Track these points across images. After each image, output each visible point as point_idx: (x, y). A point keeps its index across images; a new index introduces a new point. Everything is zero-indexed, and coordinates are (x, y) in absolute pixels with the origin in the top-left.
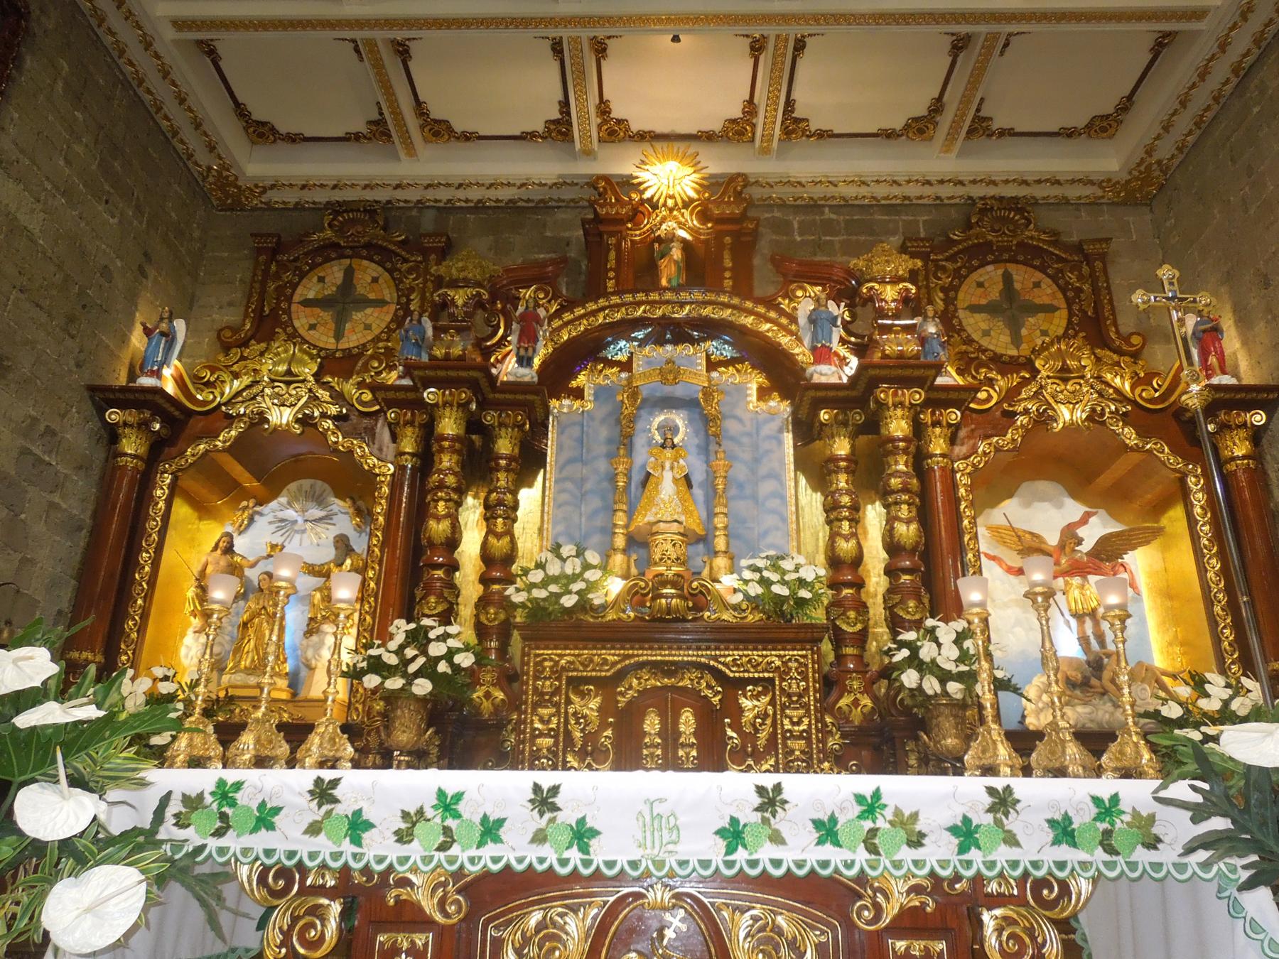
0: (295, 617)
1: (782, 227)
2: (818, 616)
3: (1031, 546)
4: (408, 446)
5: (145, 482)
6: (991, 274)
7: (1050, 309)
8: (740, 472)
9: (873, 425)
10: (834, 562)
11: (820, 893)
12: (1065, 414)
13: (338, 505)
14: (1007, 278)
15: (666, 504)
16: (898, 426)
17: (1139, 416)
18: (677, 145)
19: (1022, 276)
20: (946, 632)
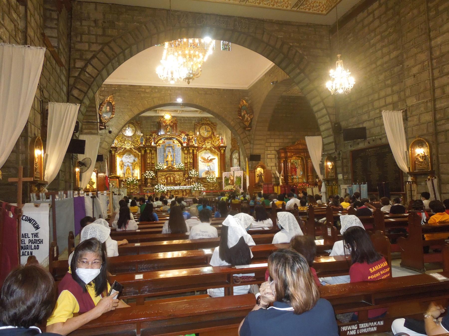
0: (131, 168)
1: (181, 120)
2: (183, 169)
3: (204, 159)
4: (143, 152)
5: (115, 155)
6: (204, 126)
7: (210, 131)
8: (176, 154)
9: (189, 150)
10: (185, 163)
11: (182, 190)
12: (208, 147)
13: (132, 155)
14: (205, 128)
15: (170, 159)
16: (191, 151)
17: (215, 148)
18: (169, 112)
19: (207, 127)
20: (193, 170)
